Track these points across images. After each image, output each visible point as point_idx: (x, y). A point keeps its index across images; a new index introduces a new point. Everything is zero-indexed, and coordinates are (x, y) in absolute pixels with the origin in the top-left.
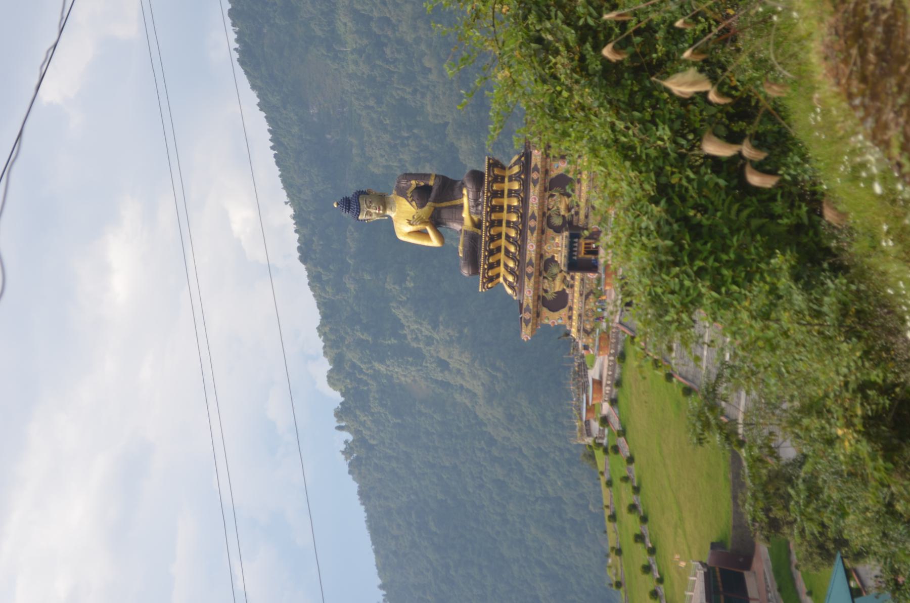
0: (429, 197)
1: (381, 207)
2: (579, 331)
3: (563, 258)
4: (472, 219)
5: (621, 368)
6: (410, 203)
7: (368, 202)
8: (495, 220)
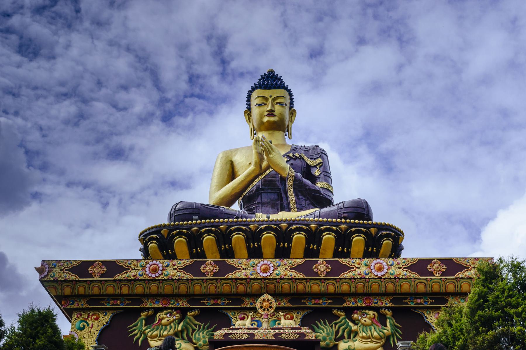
3: (246, 331)
8: (290, 241)
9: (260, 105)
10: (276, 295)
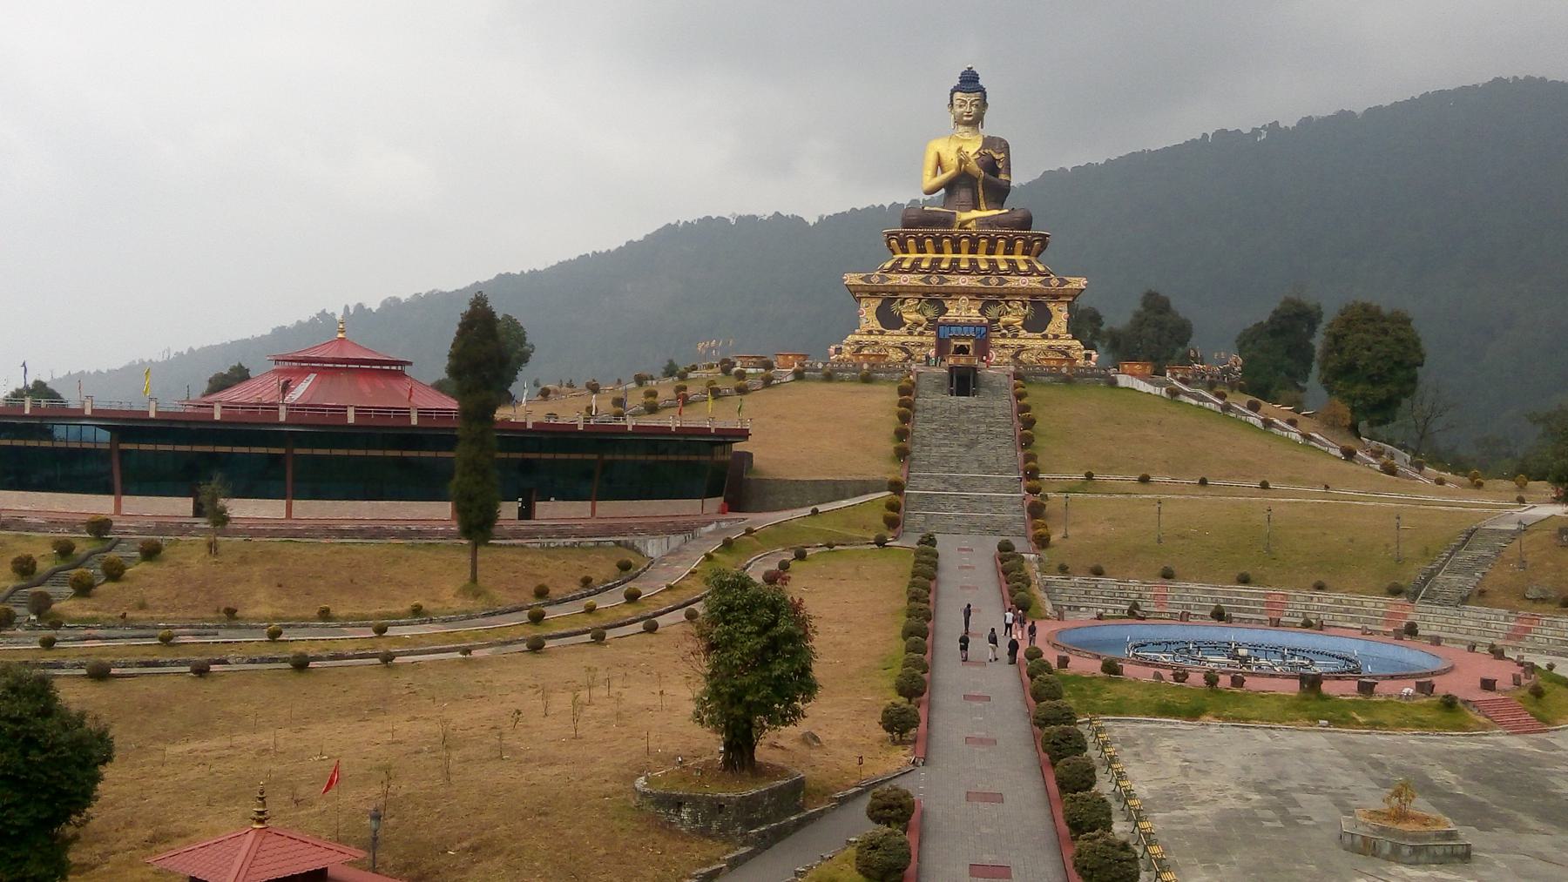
1: (970, 119)
2: (857, 342)
4: (969, 221)
6: (978, 152)
7: (976, 102)
8: (978, 244)
9: (961, 106)
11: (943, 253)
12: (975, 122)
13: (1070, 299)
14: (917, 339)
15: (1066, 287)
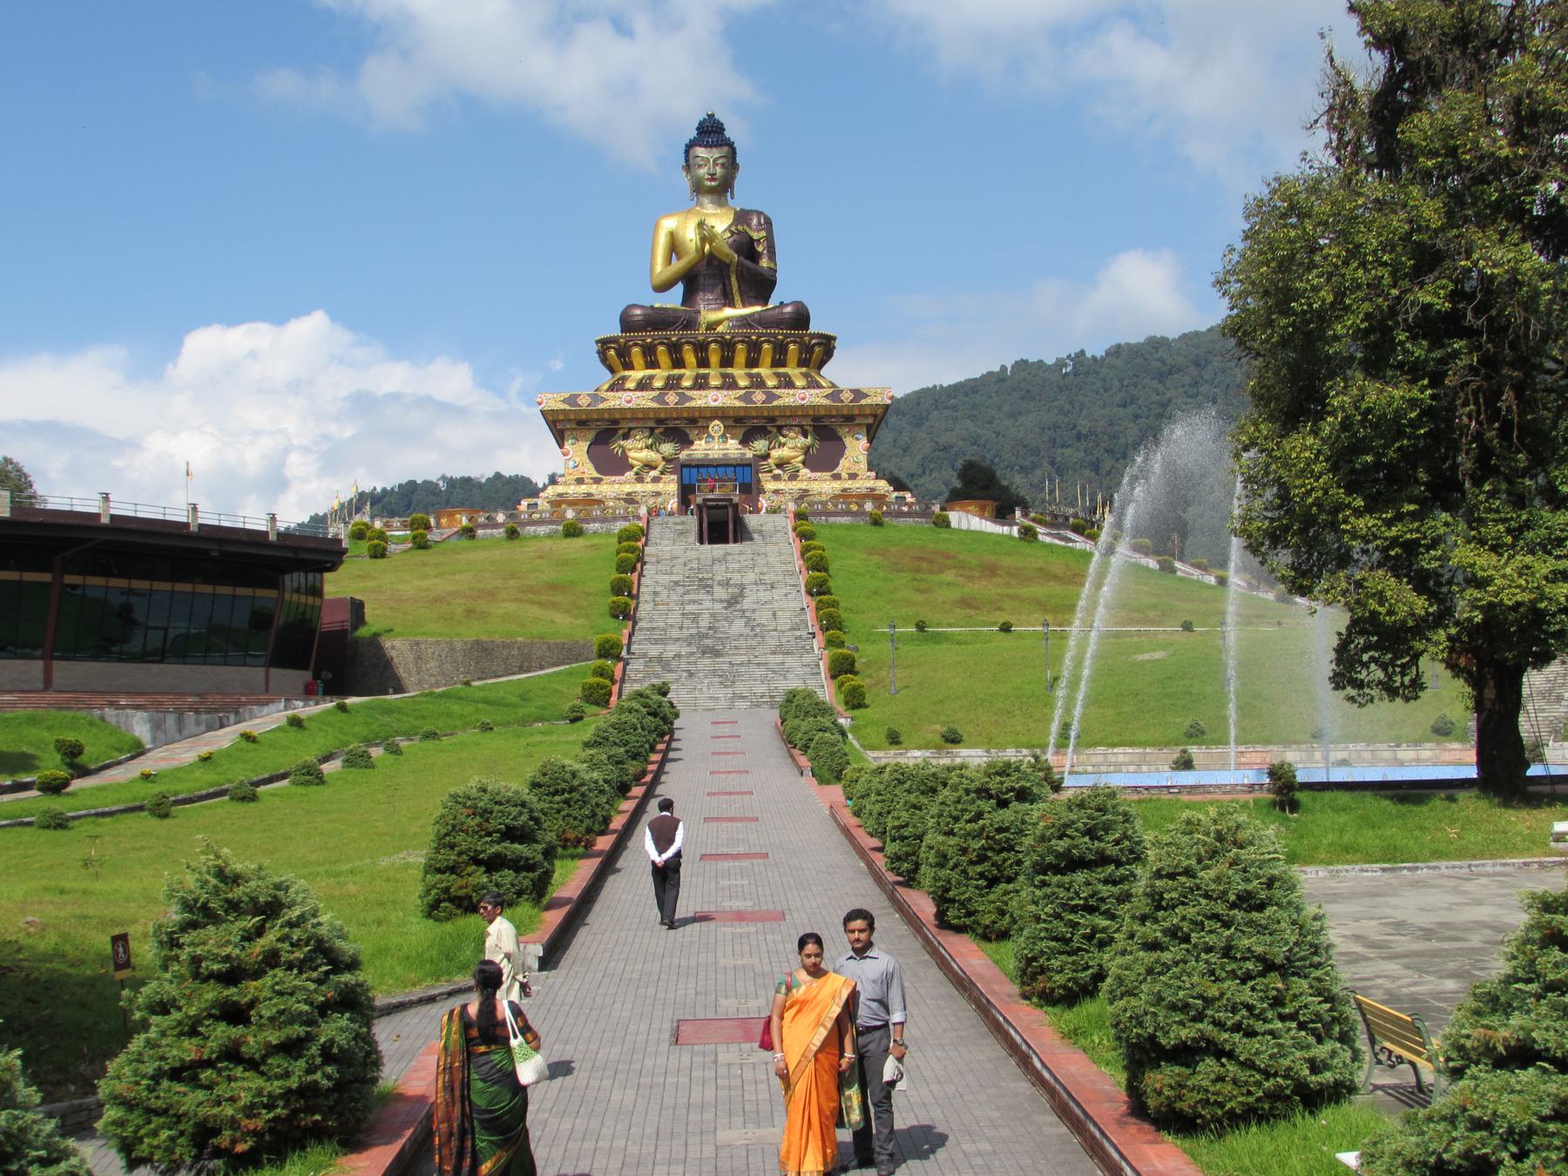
0: (746, 258)
4: (719, 322)
5: (549, 536)
6: (728, 229)
7: (720, 161)
8: (734, 352)
10: (722, 418)
11: (684, 367)
12: (722, 189)
13: (871, 421)
14: (650, 487)
15: (863, 402)
